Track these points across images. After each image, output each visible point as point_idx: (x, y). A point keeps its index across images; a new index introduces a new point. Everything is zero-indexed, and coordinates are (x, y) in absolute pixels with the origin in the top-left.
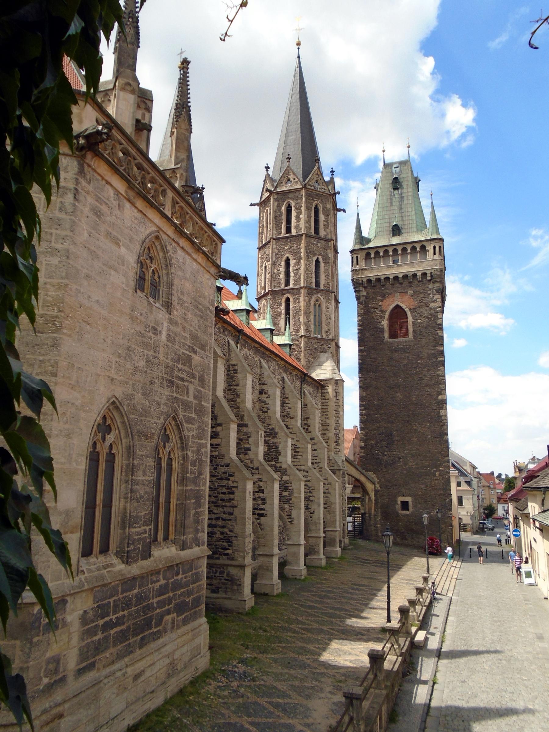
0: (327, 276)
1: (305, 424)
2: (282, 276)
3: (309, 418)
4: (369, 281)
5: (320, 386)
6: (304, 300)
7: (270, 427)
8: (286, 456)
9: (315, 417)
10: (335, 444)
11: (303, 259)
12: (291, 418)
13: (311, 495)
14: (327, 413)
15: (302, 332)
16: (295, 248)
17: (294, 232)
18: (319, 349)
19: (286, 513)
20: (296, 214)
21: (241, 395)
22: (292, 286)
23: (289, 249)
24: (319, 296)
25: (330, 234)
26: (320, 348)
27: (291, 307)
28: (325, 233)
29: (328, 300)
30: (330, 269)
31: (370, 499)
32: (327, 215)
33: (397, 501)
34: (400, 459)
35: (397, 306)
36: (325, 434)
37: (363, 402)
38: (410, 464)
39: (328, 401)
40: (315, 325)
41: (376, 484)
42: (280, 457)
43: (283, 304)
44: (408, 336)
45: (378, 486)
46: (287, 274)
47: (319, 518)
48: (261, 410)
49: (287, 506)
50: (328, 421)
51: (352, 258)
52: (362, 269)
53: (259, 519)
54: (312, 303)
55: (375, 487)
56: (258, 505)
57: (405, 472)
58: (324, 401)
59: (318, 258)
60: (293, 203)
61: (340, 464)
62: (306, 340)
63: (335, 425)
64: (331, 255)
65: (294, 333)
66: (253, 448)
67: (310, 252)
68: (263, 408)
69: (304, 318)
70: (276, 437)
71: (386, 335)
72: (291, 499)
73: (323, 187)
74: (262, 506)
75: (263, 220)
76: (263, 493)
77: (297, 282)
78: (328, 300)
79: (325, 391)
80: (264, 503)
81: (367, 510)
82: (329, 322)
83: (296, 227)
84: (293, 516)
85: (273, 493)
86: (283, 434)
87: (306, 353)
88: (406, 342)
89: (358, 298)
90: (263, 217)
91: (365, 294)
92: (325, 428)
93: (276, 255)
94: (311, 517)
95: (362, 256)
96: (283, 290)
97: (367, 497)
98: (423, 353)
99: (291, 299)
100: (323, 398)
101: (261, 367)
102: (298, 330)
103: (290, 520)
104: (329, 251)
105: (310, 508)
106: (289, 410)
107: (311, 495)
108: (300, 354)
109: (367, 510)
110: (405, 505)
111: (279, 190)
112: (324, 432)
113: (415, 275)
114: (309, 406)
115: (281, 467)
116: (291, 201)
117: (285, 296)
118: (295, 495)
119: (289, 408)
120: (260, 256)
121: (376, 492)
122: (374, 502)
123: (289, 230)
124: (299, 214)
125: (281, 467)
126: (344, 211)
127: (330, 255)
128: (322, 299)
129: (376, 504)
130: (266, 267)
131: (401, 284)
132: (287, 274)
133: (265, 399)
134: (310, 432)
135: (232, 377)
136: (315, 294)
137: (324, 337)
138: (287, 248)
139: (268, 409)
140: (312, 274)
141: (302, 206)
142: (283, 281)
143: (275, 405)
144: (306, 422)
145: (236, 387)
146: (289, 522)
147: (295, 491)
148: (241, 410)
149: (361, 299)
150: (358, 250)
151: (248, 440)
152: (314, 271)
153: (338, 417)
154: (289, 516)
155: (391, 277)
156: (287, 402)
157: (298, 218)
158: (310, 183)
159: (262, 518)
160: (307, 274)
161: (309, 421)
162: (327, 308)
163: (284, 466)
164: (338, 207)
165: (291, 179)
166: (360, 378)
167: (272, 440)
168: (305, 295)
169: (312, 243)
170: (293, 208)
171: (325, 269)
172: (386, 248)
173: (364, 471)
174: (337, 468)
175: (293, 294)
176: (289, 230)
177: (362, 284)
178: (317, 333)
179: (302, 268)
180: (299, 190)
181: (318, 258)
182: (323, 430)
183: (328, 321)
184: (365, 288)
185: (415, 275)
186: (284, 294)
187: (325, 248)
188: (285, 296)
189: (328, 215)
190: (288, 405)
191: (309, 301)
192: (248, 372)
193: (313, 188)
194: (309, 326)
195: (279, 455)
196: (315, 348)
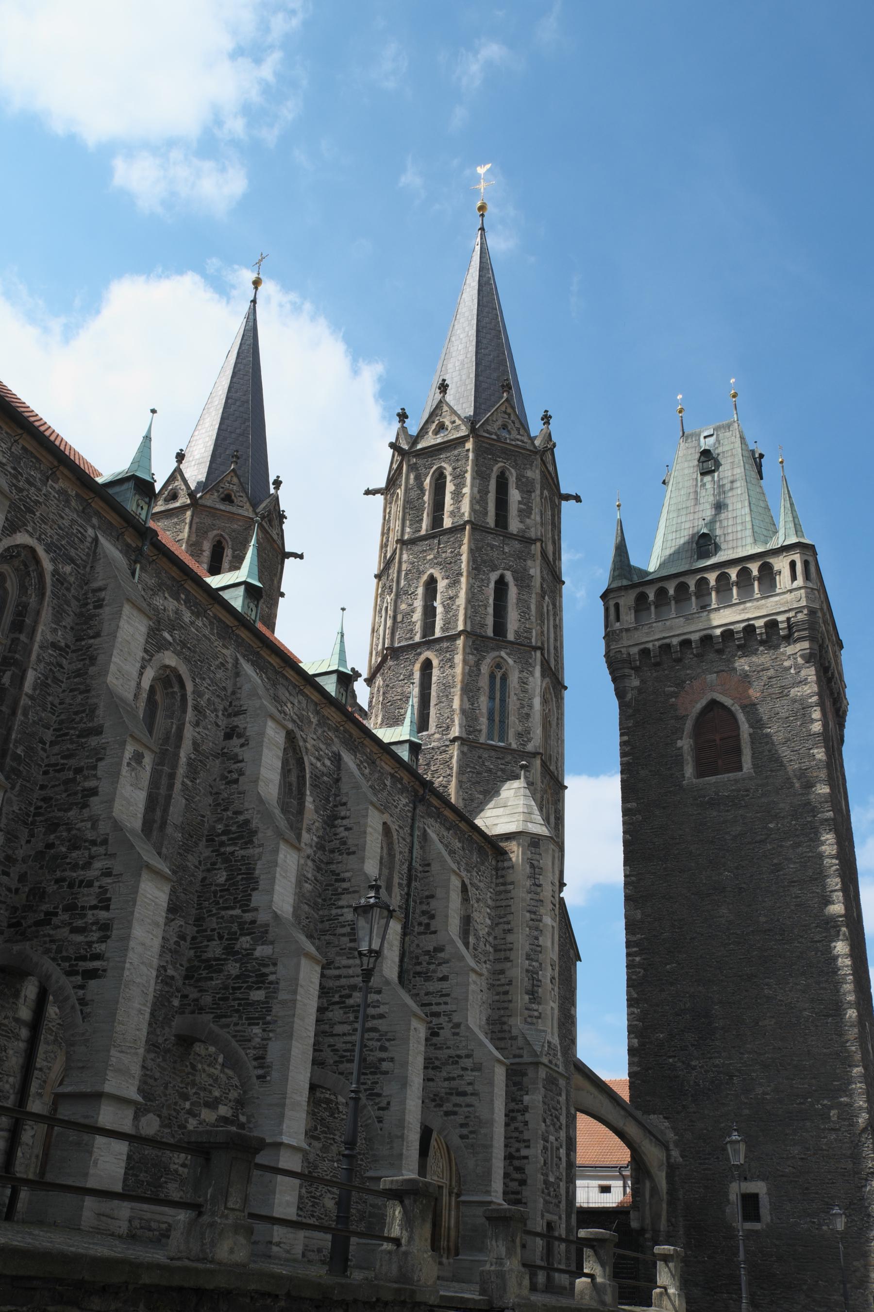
0: (524, 614)
1: (424, 913)
2: (417, 616)
3: (432, 896)
4: (645, 652)
5: (493, 847)
6: (465, 661)
7: (241, 818)
8: (270, 892)
9: (448, 893)
10: (527, 997)
11: (465, 574)
12: (349, 854)
13: (384, 1055)
14: (510, 917)
15: (455, 731)
16: (448, 555)
17: (447, 523)
18: (499, 773)
19: (252, 1052)
20: (453, 488)
21: (99, 658)
22: (438, 634)
23: (435, 558)
24: (503, 654)
25: (533, 529)
26: (503, 770)
27: (434, 679)
28: (521, 526)
29: (526, 667)
30: (533, 601)
31: (654, 1190)
32: (526, 488)
33: (726, 1194)
34: (731, 1077)
35: (713, 704)
36: (502, 972)
37: (634, 934)
38: (759, 1090)
39: (511, 887)
40: (491, 718)
41: (671, 1146)
42: (254, 894)
43: (417, 675)
44: (740, 769)
45: (675, 1153)
46: (429, 612)
47: (401, 1123)
48: (223, 777)
49: (257, 1030)
50: (510, 938)
51: (607, 610)
52: (628, 630)
53: (82, 987)
54: (485, 669)
55: (669, 1157)
56: (90, 944)
57: (747, 1112)
58: (502, 888)
59: (502, 577)
60: (448, 470)
61: (538, 1049)
62: (465, 749)
63: (527, 948)
64: (535, 570)
65: (437, 736)
66: (104, 787)
67: (484, 562)
68: (230, 772)
69: (462, 700)
70: (251, 842)
71: (689, 770)
72: (269, 1010)
73: (519, 437)
74: (99, 948)
75: (390, 517)
76: (107, 908)
77: (448, 623)
78: (526, 667)
79: (506, 864)
80: (104, 939)
81: (648, 1221)
82: (528, 715)
83: (453, 514)
84: (269, 1058)
85: (134, 904)
86: (269, 833)
87: (465, 778)
88: (736, 781)
89: (620, 694)
90: (390, 513)
91: (636, 683)
92: (502, 955)
93: (406, 574)
94: (380, 1120)
95: (627, 600)
96: (418, 645)
97: (648, 1184)
98: (781, 805)
99: (435, 662)
100: (501, 880)
101: (237, 674)
102: (448, 728)
103: (260, 1072)
104: (529, 563)
105: (379, 1095)
106: (344, 834)
107: (384, 1055)
108: (449, 782)
109: (648, 1221)
110: (750, 1202)
111: (419, 446)
112: (499, 967)
113: (750, 630)
114: (435, 867)
115: (253, 922)
116: (443, 464)
117: (422, 658)
118: (283, 996)
119: (347, 829)
120: (380, 590)
121: (672, 1169)
122: (665, 1197)
123: (437, 520)
124: (459, 486)
125: (253, 922)
126: (578, 499)
127: (532, 572)
128: (510, 661)
129: (669, 1203)
130: (387, 608)
131: (720, 652)
132: (429, 612)
133: (237, 750)
134: (435, 932)
135: (92, 617)
136: (493, 649)
137: (514, 746)
138: (432, 556)
139: (241, 773)
140: (486, 606)
141: (466, 472)
142: (418, 627)
143: (257, 762)
144: (424, 907)
145: (91, 641)
146: (259, 1077)
147: (282, 985)
148: (93, 693)
149: (629, 696)
150: (620, 589)
151: (95, 768)
152: (491, 601)
153: (537, 929)
154: (260, 1059)
155: (695, 637)
156: (343, 814)
157: (457, 495)
158: (489, 428)
159: (92, 983)
160: (473, 607)
161: (434, 903)
162: (523, 682)
163: (263, 917)
164: (564, 491)
165: (447, 423)
166: (625, 876)
167: (242, 852)
168: (468, 650)
169: (488, 545)
170: (449, 478)
171: (519, 600)
172: (682, 579)
173: (639, 1114)
174: (530, 1060)
175: (440, 651)
176: (437, 520)
177: (628, 661)
178: (496, 738)
179: (462, 594)
180: (462, 441)
181: (502, 577)
182: (498, 960)
183: (525, 710)
184: (636, 669)
185: (750, 630)
186: (420, 654)
187: (522, 557)
188: (422, 658)
189: (530, 492)
190: (345, 822)
191: (478, 664)
192: (128, 600)
193: (494, 437)
194: (476, 719)
195: (254, 889)
196: (490, 771)
